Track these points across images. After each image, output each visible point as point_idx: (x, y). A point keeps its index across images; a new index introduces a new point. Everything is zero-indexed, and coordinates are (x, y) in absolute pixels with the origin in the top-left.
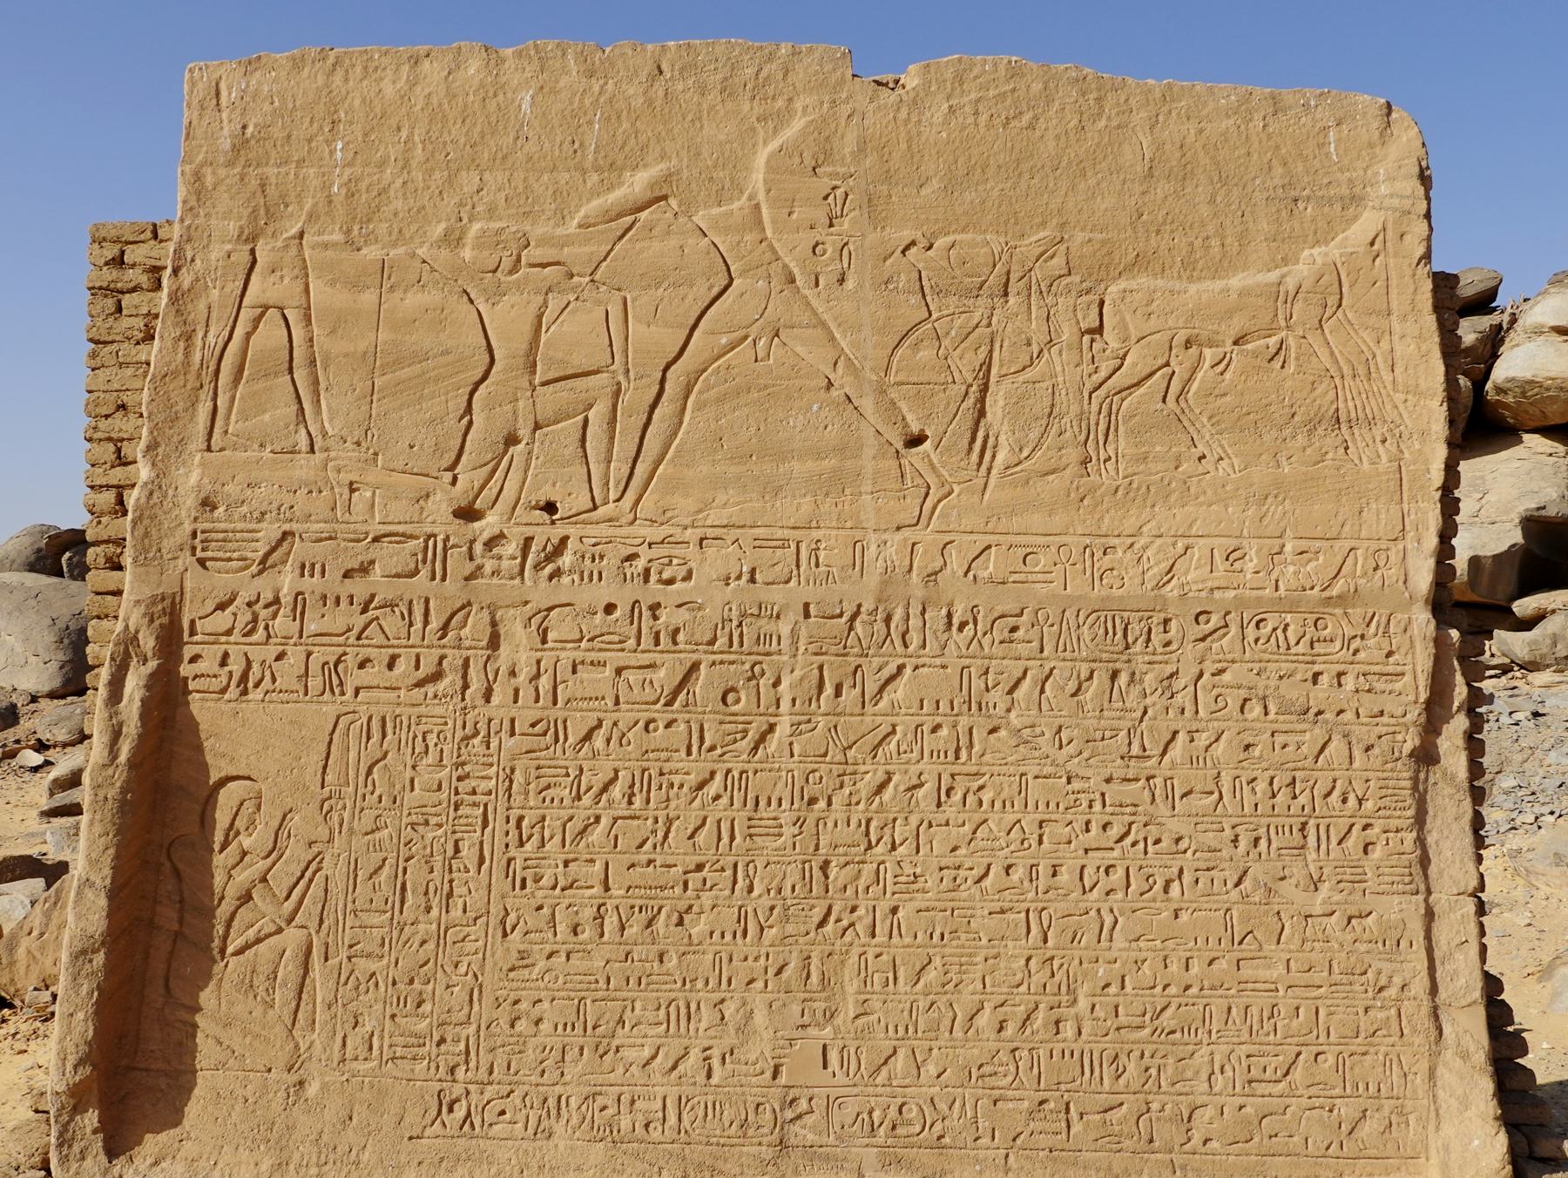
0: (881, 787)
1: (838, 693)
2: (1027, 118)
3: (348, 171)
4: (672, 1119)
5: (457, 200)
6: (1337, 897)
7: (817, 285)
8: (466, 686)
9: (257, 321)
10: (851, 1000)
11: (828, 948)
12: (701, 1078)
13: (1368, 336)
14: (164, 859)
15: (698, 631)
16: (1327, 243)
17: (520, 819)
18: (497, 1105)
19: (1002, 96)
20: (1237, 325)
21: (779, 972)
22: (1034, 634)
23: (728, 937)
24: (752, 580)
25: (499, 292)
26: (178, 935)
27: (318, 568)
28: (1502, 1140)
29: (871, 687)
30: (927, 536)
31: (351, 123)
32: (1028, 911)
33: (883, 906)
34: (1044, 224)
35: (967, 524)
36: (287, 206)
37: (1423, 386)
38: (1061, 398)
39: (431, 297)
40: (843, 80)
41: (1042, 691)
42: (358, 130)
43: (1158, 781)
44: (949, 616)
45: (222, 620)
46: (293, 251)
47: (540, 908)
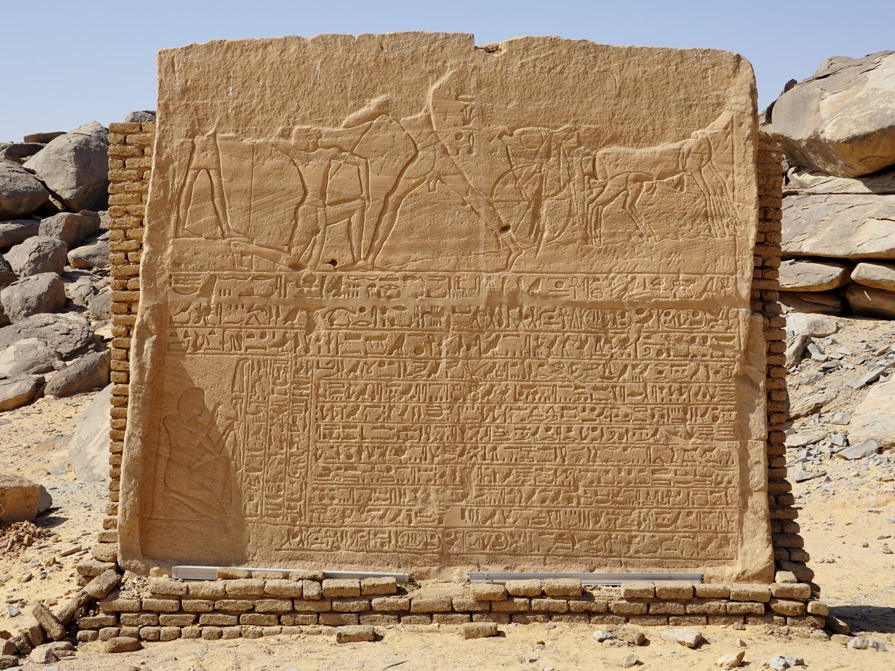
0: (488, 393)
1: (468, 349)
2: (559, 68)
3: (236, 101)
4: (393, 542)
5: (287, 115)
6: (699, 441)
7: (458, 153)
8: (296, 347)
9: (195, 176)
10: (474, 488)
11: (463, 466)
12: (406, 523)
13: (722, 174)
14: (161, 425)
15: (403, 320)
16: (705, 127)
17: (322, 407)
18: (316, 535)
19: (546, 58)
20: (659, 169)
21: (441, 477)
22: (560, 319)
23: (418, 461)
24: (428, 296)
25: (308, 159)
26: (170, 460)
27: (227, 291)
28: (770, 550)
29: (483, 345)
30: (509, 274)
31: (236, 78)
32: (556, 448)
33: (489, 446)
34: (567, 121)
35: (529, 267)
36: (207, 119)
37: (746, 200)
38: (574, 207)
39: (277, 161)
40: (470, 50)
41: (564, 347)
42: (239, 81)
43: (618, 389)
44: (520, 311)
45: (184, 316)
46: (212, 141)
47: (332, 447)
